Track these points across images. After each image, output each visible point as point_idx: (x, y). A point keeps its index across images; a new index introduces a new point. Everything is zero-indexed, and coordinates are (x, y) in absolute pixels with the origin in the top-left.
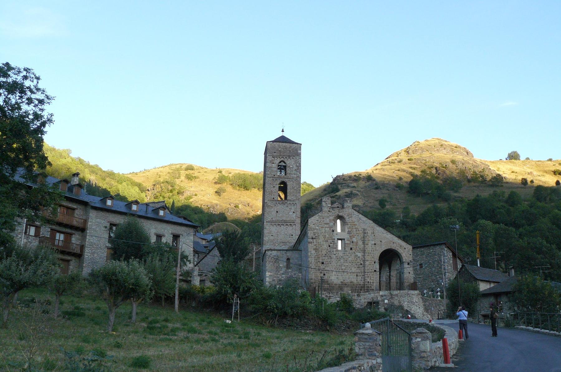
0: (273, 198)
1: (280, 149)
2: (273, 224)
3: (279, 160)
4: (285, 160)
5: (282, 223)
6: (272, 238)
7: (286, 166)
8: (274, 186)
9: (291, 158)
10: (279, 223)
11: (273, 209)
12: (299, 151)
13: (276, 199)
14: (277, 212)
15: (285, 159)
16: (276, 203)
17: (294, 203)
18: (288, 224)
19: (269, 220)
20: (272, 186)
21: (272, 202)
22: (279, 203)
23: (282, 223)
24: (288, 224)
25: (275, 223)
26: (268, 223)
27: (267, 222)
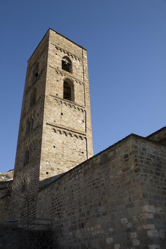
0: (57, 95)
1: (64, 44)
2: (56, 128)
3: (63, 55)
4: (70, 57)
6: (54, 151)
8: (58, 79)
11: (55, 109)
14: (62, 114)
16: (62, 102)
17: (84, 109)
19: (51, 121)
20: (55, 79)
21: (55, 98)
23: (69, 132)
24: (77, 134)
26: (49, 126)
27: (47, 124)
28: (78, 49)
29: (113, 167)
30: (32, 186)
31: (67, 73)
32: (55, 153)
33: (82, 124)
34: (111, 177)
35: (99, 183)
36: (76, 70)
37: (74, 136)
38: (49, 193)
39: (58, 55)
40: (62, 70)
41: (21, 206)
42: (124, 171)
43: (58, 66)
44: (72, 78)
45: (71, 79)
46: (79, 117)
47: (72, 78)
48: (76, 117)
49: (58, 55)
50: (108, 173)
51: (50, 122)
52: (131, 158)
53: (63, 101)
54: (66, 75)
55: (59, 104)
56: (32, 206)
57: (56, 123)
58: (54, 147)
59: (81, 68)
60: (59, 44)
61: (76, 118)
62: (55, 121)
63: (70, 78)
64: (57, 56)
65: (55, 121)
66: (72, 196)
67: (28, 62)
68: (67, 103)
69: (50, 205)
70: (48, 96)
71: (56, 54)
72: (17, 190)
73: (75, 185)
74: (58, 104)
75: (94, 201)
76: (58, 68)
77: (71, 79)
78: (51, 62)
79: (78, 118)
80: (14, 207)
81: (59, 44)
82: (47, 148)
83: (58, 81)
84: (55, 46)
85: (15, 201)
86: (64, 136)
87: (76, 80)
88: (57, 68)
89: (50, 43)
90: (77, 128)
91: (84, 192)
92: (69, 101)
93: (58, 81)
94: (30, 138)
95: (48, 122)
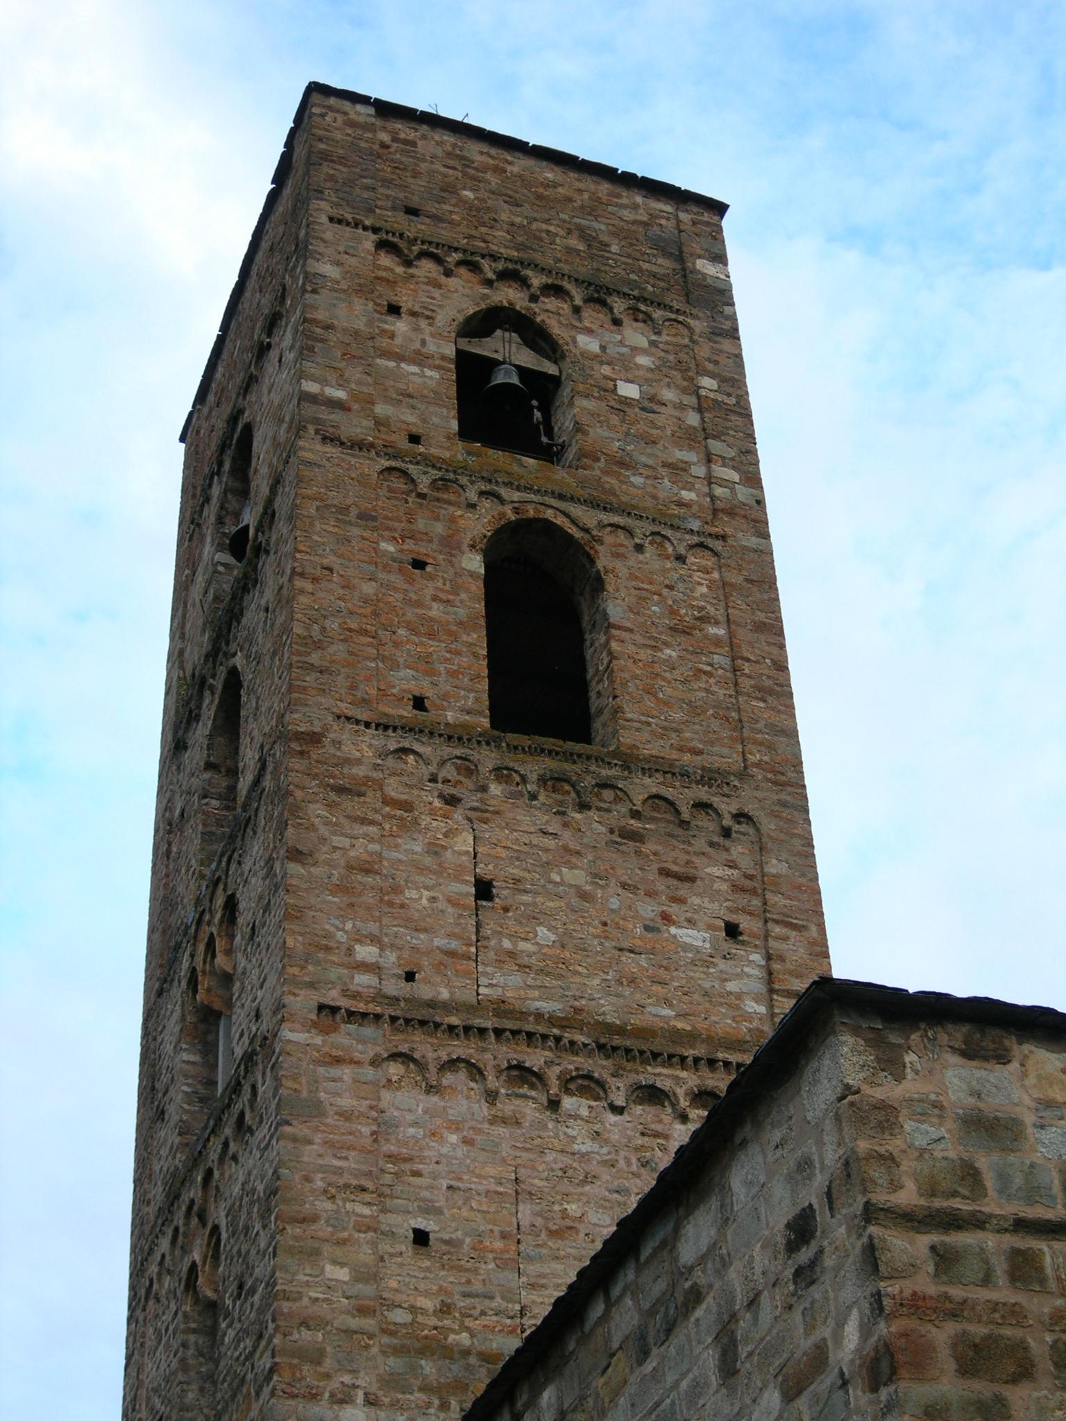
0: (419, 703)
2: (426, 1048)
5: (572, 1063)
7: (556, 381)
8: (422, 550)
9: (619, 305)
10: (535, 1058)
12: (705, 267)
13: (450, 716)
14: (484, 890)
15: (551, 303)
16: (468, 768)
18: (662, 1076)
22: (501, 773)
24: (662, 1076)
25: (459, 1048)
28: (627, 214)
31: (516, 468)
32: (428, 1304)
33: (722, 965)
36: (615, 420)
37: (640, 1101)
39: (413, 314)
40: (458, 451)
43: (411, 418)
44: (577, 511)
45: (567, 515)
46: (683, 890)
47: (577, 511)
48: (650, 894)
49: (413, 314)
51: (356, 996)
53: (487, 758)
54: (503, 492)
55: (448, 790)
57: (426, 989)
58: (421, 1238)
59: (669, 395)
60: (412, 211)
61: (648, 910)
62: (410, 977)
63: (549, 514)
64: (401, 326)
65: (410, 977)
67: (182, 439)
68: (533, 768)
70: (326, 729)
71: (394, 310)
74: (441, 796)
76: (415, 439)
77: (560, 521)
78: (340, 394)
79: (674, 909)
81: (412, 211)
82: (335, 1262)
83: (419, 564)
84: (375, 230)
86: (530, 1110)
87: (616, 519)
88: (405, 444)
89: (324, 219)
90: (667, 1012)
92: (549, 742)
93: (419, 564)
95: (333, 996)
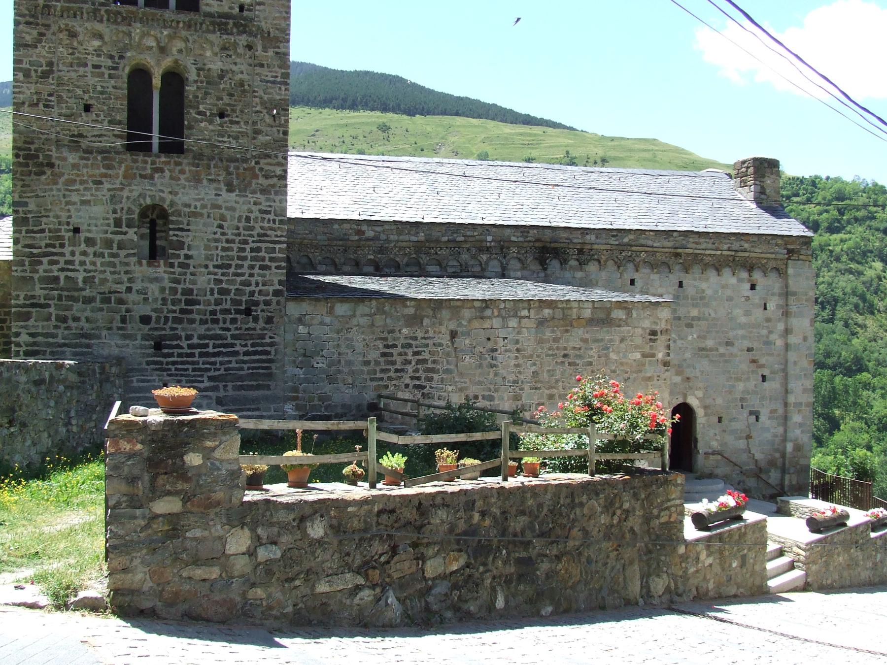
29: (622, 340)
30: (233, 263)
34: (613, 356)
35: (580, 357)
38: (364, 321)
41: (146, 310)
42: (644, 356)
50: (608, 348)
52: (662, 339)
56: (237, 329)
66: (489, 359)
69: (373, 355)
72: (82, 236)
73: (505, 339)
75: (561, 388)
80: (75, 300)
85: (80, 276)
91: (535, 364)
94: (171, 37)
